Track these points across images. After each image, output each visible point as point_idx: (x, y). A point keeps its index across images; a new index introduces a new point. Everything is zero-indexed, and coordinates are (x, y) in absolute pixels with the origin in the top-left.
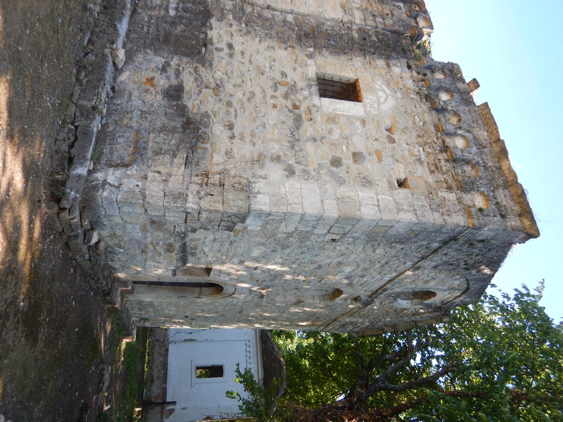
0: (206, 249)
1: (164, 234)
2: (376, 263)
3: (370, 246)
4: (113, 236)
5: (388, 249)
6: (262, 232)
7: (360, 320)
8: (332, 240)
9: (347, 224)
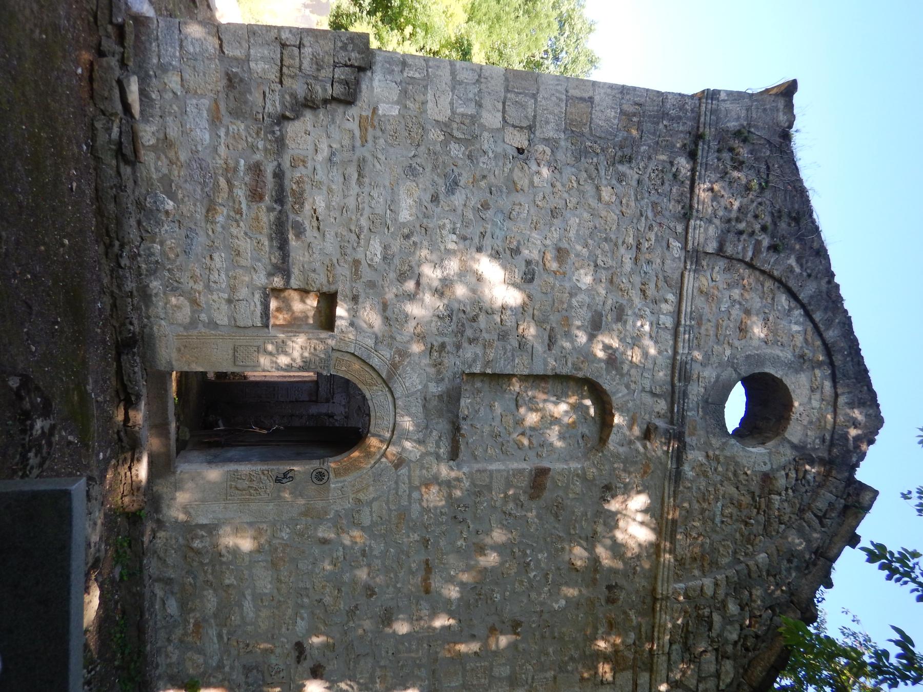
0: (320, 203)
1: (247, 128)
2: (622, 250)
3: (585, 175)
4: (165, 143)
5: (620, 189)
6: (403, 123)
7: (708, 582)
8: (520, 151)
9: (526, 95)
